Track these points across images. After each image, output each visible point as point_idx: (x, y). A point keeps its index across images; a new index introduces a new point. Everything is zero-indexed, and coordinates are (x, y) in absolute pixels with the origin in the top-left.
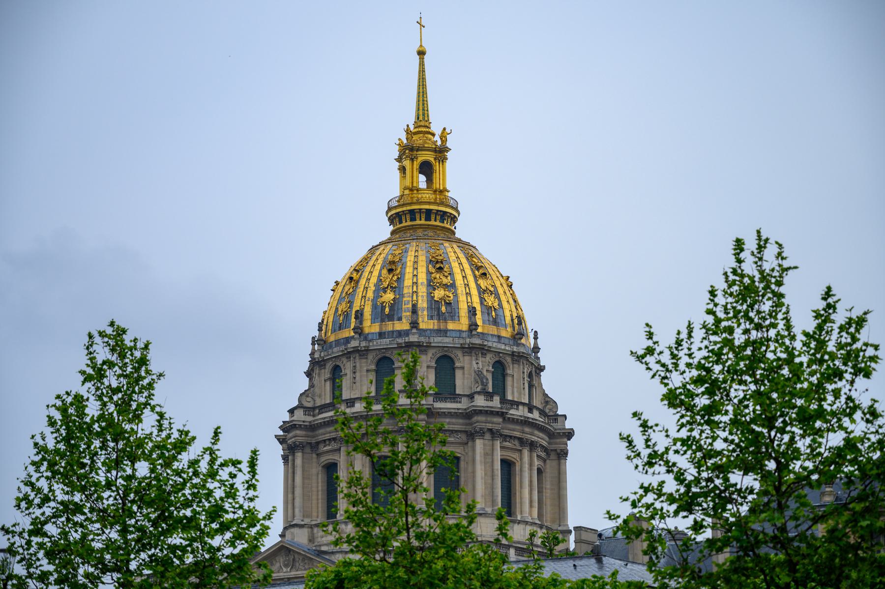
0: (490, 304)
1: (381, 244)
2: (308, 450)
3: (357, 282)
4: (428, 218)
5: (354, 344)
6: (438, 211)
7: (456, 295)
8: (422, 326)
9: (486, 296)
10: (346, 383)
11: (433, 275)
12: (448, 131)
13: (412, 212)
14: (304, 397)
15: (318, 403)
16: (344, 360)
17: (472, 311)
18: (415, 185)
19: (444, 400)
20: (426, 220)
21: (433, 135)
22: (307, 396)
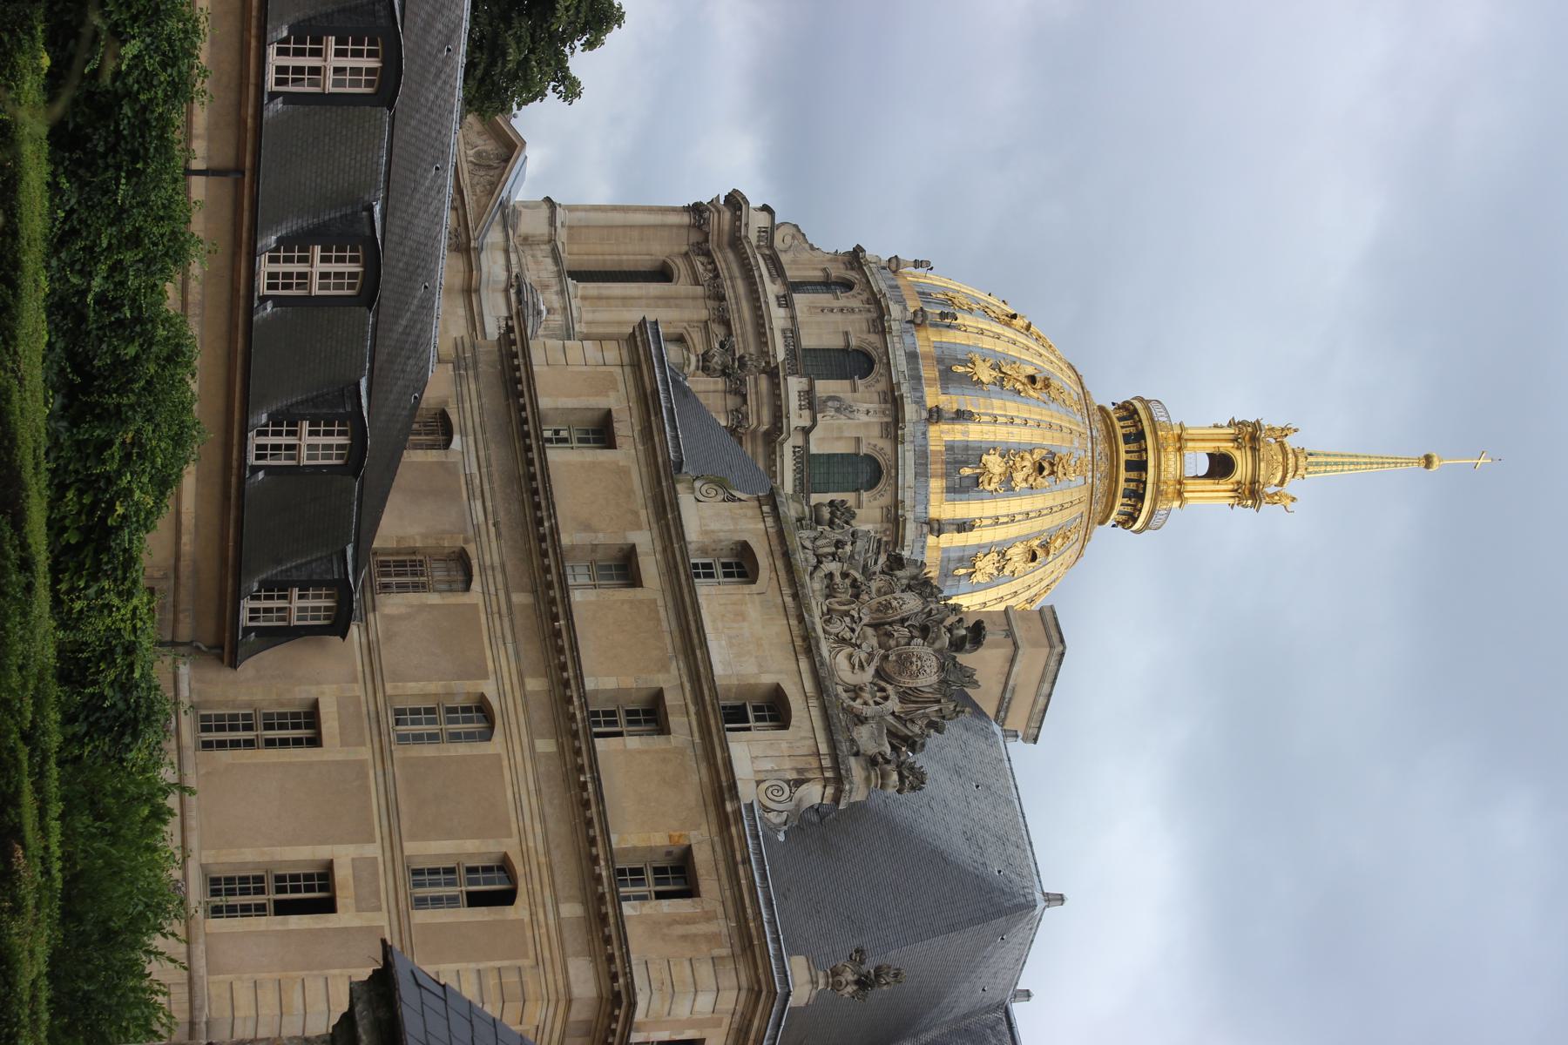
0: (979, 564)
1: (1079, 378)
2: (695, 237)
3: (1008, 325)
4: (1130, 466)
5: (895, 310)
6: (1145, 483)
7: (993, 494)
8: (934, 431)
9: (994, 556)
10: (824, 299)
11: (1027, 456)
12: (1291, 506)
13: (1141, 436)
14: (793, 230)
15: (784, 258)
16: (865, 296)
17: (963, 526)
18: (1190, 444)
19: (799, 471)
20: (1127, 462)
21: (1282, 482)
22: (793, 237)
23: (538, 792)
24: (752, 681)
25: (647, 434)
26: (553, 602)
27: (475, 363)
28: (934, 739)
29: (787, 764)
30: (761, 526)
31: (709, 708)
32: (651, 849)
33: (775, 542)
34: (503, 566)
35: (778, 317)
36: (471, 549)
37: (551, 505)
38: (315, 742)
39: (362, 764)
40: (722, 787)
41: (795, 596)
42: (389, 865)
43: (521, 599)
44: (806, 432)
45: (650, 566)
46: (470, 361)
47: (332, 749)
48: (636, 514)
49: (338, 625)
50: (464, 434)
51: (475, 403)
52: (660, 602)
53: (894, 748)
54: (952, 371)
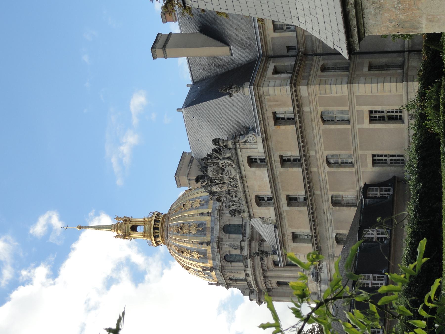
5: (218, 272)
6: (154, 224)
7: (194, 222)
8: (209, 239)
15: (247, 287)
16: (226, 276)
17: (202, 214)
19: (245, 230)
21: (118, 223)
22: (244, 292)
23: (314, 141)
24: (257, 169)
25: (283, 236)
26: (310, 191)
27: (329, 256)
28: (210, 152)
29: (248, 147)
30: (254, 210)
31: (269, 162)
32: (285, 125)
33: (250, 206)
34: (323, 202)
35: (249, 271)
36: (331, 206)
37: (309, 218)
38: (373, 156)
39: (361, 150)
40: (265, 140)
41: (245, 191)
42: (354, 122)
43: (318, 193)
44: (243, 240)
45: (284, 201)
46: (330, 257)
47: (369, 154)
48: (287, 215)
49: (366, 187)
50: (332, 237)
51: (329, 245)
52: (281, 190)
53: (220, 150)
54: (204, 256)
